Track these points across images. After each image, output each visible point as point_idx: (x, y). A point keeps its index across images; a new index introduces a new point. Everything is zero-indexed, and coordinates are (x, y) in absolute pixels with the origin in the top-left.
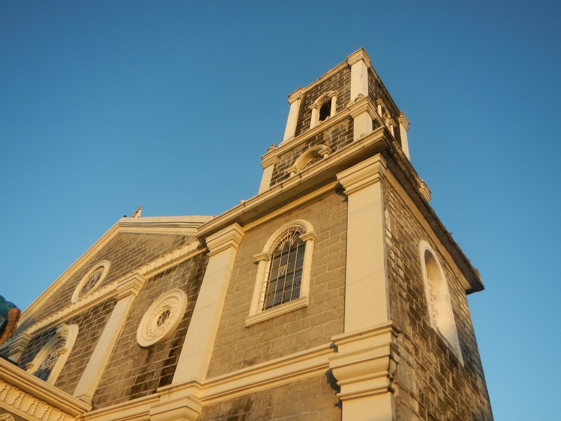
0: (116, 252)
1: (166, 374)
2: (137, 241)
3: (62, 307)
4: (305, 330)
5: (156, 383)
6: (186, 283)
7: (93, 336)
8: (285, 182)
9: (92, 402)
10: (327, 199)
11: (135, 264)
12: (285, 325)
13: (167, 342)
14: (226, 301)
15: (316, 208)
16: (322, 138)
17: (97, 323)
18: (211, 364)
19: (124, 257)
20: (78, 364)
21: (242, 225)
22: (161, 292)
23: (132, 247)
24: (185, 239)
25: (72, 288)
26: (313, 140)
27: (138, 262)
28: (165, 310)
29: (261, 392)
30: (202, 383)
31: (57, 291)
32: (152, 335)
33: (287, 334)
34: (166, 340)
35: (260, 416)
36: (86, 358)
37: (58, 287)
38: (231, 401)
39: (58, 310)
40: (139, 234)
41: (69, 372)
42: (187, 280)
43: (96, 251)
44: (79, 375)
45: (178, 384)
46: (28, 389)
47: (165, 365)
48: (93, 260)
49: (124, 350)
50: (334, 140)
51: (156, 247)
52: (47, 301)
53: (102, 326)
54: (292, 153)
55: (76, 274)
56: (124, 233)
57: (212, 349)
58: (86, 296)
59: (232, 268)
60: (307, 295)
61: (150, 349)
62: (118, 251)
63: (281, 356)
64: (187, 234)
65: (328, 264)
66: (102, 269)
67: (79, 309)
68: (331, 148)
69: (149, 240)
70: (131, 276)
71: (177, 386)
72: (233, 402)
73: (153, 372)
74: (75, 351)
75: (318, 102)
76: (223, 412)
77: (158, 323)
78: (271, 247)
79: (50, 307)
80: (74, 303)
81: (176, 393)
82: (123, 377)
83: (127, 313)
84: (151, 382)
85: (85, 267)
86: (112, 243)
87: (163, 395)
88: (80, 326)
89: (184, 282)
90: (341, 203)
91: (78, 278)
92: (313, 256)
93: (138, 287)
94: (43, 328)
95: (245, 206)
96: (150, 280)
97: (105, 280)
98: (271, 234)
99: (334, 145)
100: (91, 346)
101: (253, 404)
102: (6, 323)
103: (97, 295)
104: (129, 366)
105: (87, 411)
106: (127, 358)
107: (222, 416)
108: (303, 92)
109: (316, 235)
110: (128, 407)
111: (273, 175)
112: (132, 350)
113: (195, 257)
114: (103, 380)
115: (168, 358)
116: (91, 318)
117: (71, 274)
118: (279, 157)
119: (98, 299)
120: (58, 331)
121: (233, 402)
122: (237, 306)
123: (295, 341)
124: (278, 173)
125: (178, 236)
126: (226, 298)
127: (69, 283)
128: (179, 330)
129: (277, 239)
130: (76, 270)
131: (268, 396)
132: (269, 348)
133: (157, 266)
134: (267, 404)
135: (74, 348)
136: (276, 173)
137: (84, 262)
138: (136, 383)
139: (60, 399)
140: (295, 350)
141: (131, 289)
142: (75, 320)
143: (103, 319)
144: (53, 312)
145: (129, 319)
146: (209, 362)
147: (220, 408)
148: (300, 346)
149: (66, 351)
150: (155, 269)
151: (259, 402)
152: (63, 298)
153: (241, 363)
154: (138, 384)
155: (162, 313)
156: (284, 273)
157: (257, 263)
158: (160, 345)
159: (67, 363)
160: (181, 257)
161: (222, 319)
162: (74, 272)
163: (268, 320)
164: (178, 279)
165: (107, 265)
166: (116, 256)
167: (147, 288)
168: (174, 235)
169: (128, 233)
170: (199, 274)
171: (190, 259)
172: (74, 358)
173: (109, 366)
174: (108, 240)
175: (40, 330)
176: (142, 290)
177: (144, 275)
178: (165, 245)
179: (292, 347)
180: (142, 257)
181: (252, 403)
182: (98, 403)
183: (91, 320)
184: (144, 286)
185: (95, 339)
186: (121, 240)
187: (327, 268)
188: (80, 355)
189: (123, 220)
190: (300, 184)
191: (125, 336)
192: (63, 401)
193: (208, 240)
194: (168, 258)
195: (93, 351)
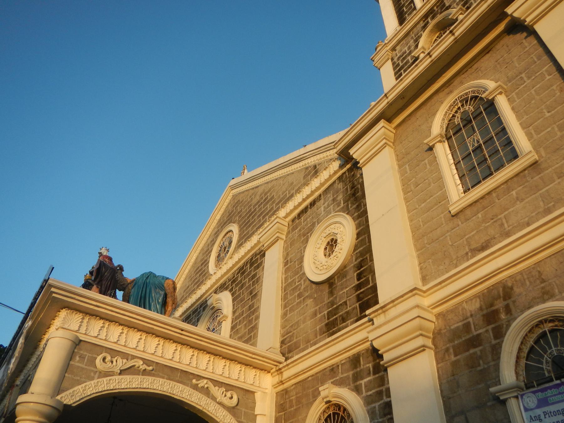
0: (239, 213)
1: (363, 298)
2: (259, 193)
3: (202, 282)
4: (551, 186)
5: (355, 311)
6: (342, 205)
7: (251, 294)
8: (455, 27)
9: (282, 353)
10: (499, 46)
11: (267, 214)
12: (514, 193)
13: (347, 268)
14: (406, 203)
15: (487, 62)
16: (444, 5)
17: (249, 281)
18: (421, 269)
19: (251, 213)
20: (245, 324)
21: (389, 120)
22: (313, 225)
23: (255, 201)
24: (317, 167)
25: (205, 263)
26: (431, 13)
27: (270, 211)
28: (329, 239)
29: (521, 273)
30: (424, 288)
31: (189, 271)
32: (325, 267)
33: (523, 200)
34: (345, 267)
35: (535, 298)
36: (254, 316)
37: (189, 267)
38: (475, 296)
39: (198, 286)
40: (258, 187)
41: (239, 335)
42: (342, 202)
43: (216, 221)
44: (252, 334)
45: (393, 298)
46: (217, 350)
47: (356, 291)
48: (216, 230)
49: (296, 294)
51: (285, 189)
52: (183, 283)
53: (257, 282)
55: (202, 249)
56: (239, 193)
57: (415, 254)
58: (225, 262)
59: (397, 167)
60: (531, 149)
61: (330, 282)
62: (241, 211)
63: (528, 224)
64: (317, 162)
66: (230, 233)
67: (222, 276)
68: (464, 7)
69: (273, 187)
70: (269, 225)
71: (393, 301)
72: (479, 297)
73: (345, 303)
74: (237, 314)
76: (471, 311)
77: (325, 255)
78: (442, 127)
79: (188, 287)
80: (215, 273)
81: (394, 308)
83: (282, 259)
84: (347, 313)
85: (211, 239)
86: (230, 208)
87: (376, 316)
88: (230, 291)
90: (524, 41)
91: (207, 252)
92: (513, 109)
93: (282, 230)
94: (190, 307)
95: (387, 98)
96: (293, 221)
97: (238, 241)
98: (434, 114)
100: (254, 303)
101: (515, 289)
102: (166, 296)
103: (236, 257)
104: (310, 306)
105: (280, 363)
106: (304, 299)
107: (472, 316)
109: (505, 87)
110: (332, 343)
111: (394, 69)
112: (305, 290)
113: (340, 178)
114: (285, 330)
115: (357, 283)
116: (239, 279)
117: (198, 252)
118: (394, 49)
119: (240, 260)
120: (209, 303)
121: (479, 297)
122: (425, 201)
123: (541, 203)
125: (307, 168)
126: (405, 199)
127: (199, 260)
128: (357, 251)
129: (445, 115)
130: (201, 246)
131: (534, 273)
132: (502, 224)
133: (296, 204)
134: (538, 282)
135: (234, 312)
137: (207, 236)
138: (328, 319)
139: (251, 355)
140: (548, 211)
141: (278, 235)
142: (223, 288)
143: (255, 275)
144: (194, 290)
145: (286, 264)
146: (418, 269)
147: (463, 309)
148: (554, 206)
149: (227, 317)
150: (296, 208)
151: (523, 284)
152: (200, 273)
153: (467, 254)
154: (331, 320)
155: (326, 243)
156: (478, 142)
157: (431, 149)
158: (341, 273)
159: (233, 328)
160: (322, 185)
161: (411, 221)
162: (200, 249)
163: (482, 198)
164: (328, 206)
165: (235, 228)
166: (240, 217)
167: (294, 229)
168: (302, 169)
169: (244, 192)
170: (355, 190)
171: (334, 182)
172: (238, 321)
173: (285, 315)
174: (224, 207)
175: (188, 310)
176: (288, 233)
177: (285, 217)
178: (295, 183)
179: (541, 210)
180: (272, 204)
181: (512, 288)
182: (290, 352)
183: (241, 281)
184: (289, 228)
185: (255, 295)
186: (239, 200)
187: (545, 111)
188: (244, 315)
189: (232, 182)
190: (456, 42)
191: (289, 281)
192: (254, 356)
193: (351, 152)
194: (307, 191)
195: (258, 307)
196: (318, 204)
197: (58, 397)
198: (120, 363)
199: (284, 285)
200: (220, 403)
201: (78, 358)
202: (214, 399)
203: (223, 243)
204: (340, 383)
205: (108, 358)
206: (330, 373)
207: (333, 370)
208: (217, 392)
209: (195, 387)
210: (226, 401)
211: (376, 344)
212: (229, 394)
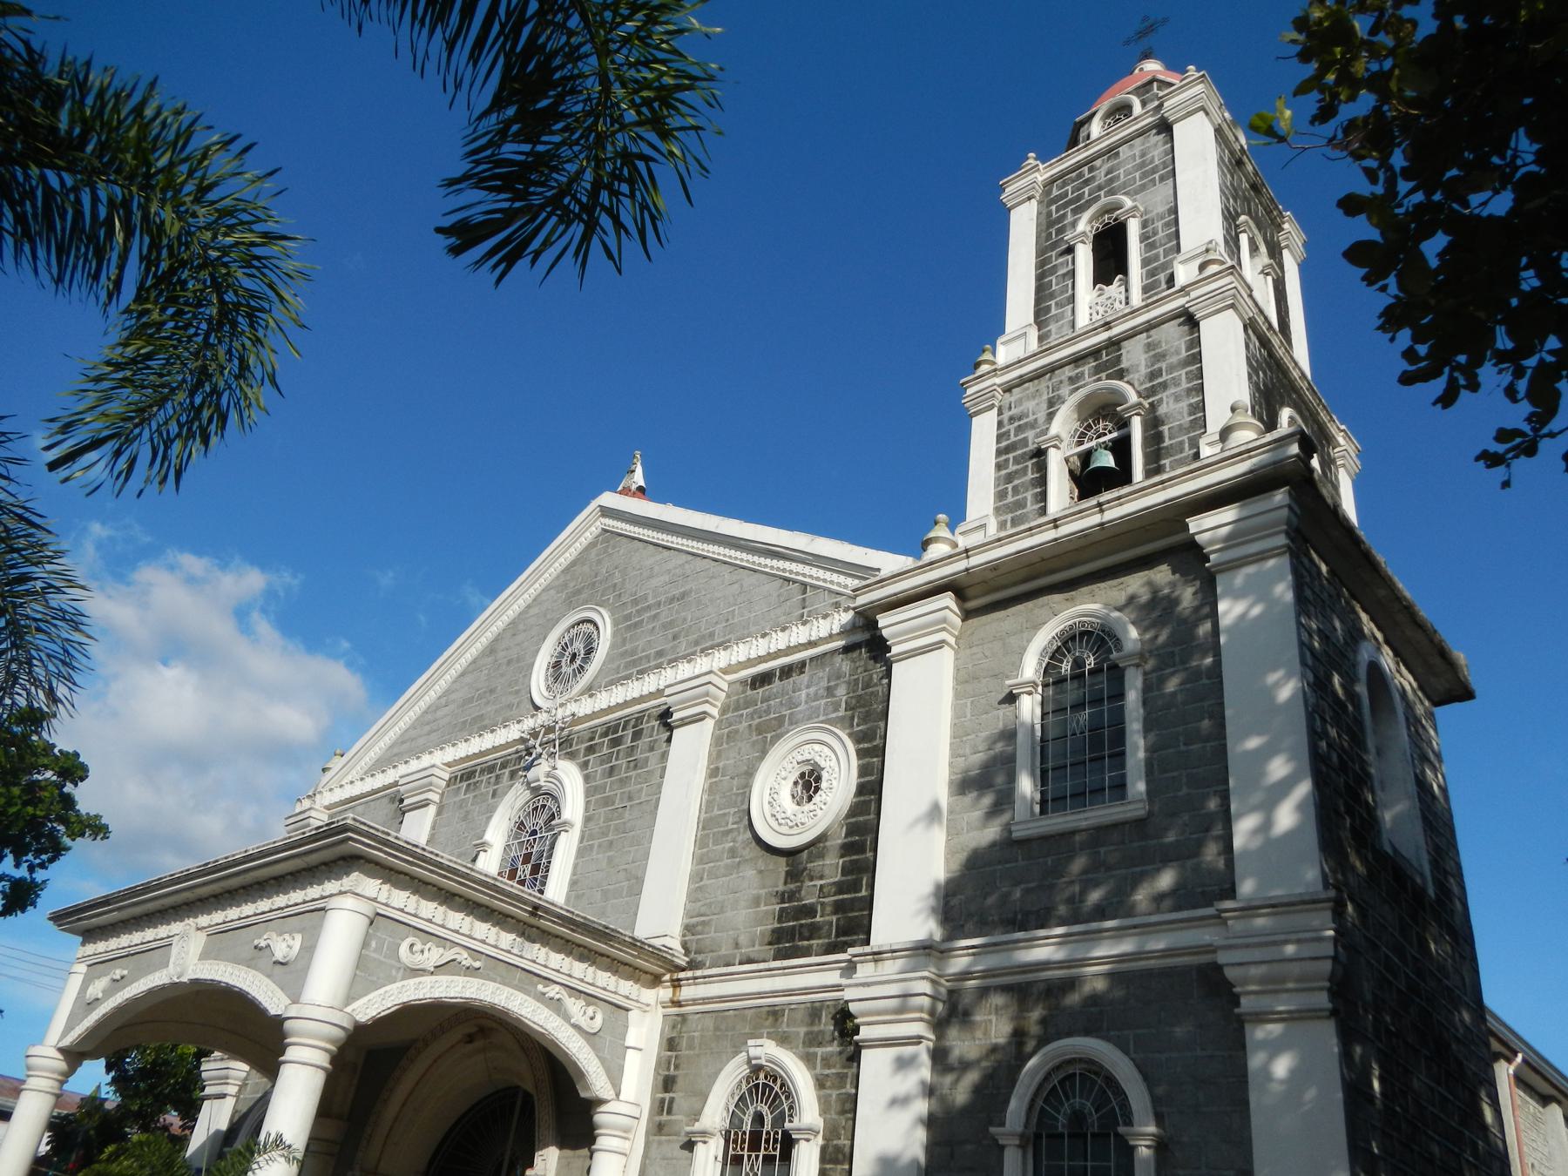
22: (780, 720)
28: (806, 768)
50: (1153, 375)
54: (1044, 383)
65: (1180, 729)
75: (1085, 225)
82: (743, 903)
88: (584, 766)
89: (836, 710)
93: (716, 699)
99: (1152, 392)
103: (604, 700)
108: (1040, 179)
118: (1008, 389)
124: (1013, 439)
135: (588, 819)
136: (1007, 434)
149: (572, 826)
164: (816, 697)
177: (725, 671)
184: (728, 696)
191: (716, 812)
193: (883, 620)
196: (795, 678)
197: (349, 1009)
198: (434, 955)
199: (703, 816)
200: (576, 1027)
201: (373, 944)
202: (566, 1017)
203: (571, 641)
204: (783, 1040)
205: (418, 947)
206: (771, 1018)
207: (775, 1013)
208: (574, 1006)
209: (541, 997)
210: (583, 1022)
211: (853, 1007)
212: (590, 1010)
